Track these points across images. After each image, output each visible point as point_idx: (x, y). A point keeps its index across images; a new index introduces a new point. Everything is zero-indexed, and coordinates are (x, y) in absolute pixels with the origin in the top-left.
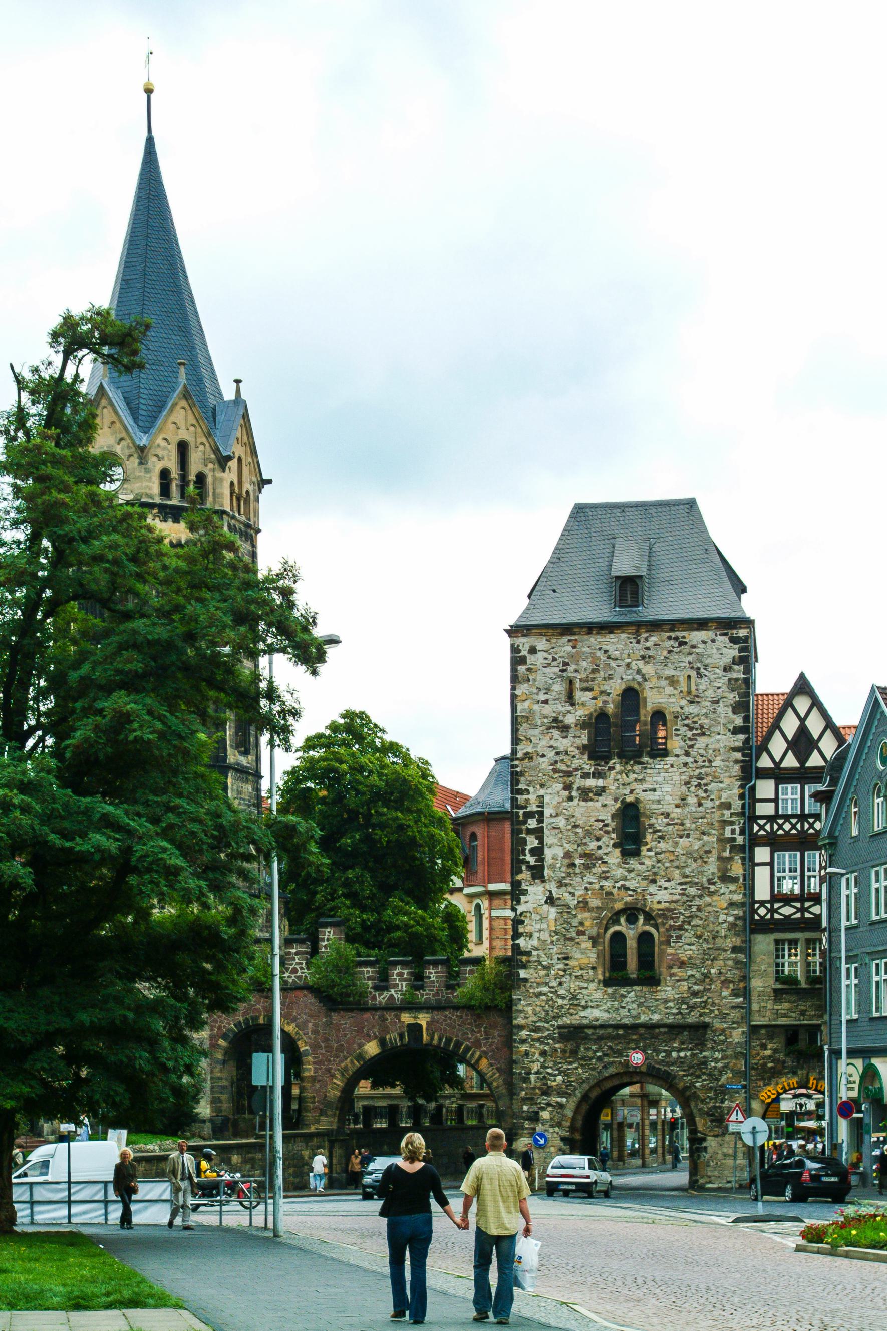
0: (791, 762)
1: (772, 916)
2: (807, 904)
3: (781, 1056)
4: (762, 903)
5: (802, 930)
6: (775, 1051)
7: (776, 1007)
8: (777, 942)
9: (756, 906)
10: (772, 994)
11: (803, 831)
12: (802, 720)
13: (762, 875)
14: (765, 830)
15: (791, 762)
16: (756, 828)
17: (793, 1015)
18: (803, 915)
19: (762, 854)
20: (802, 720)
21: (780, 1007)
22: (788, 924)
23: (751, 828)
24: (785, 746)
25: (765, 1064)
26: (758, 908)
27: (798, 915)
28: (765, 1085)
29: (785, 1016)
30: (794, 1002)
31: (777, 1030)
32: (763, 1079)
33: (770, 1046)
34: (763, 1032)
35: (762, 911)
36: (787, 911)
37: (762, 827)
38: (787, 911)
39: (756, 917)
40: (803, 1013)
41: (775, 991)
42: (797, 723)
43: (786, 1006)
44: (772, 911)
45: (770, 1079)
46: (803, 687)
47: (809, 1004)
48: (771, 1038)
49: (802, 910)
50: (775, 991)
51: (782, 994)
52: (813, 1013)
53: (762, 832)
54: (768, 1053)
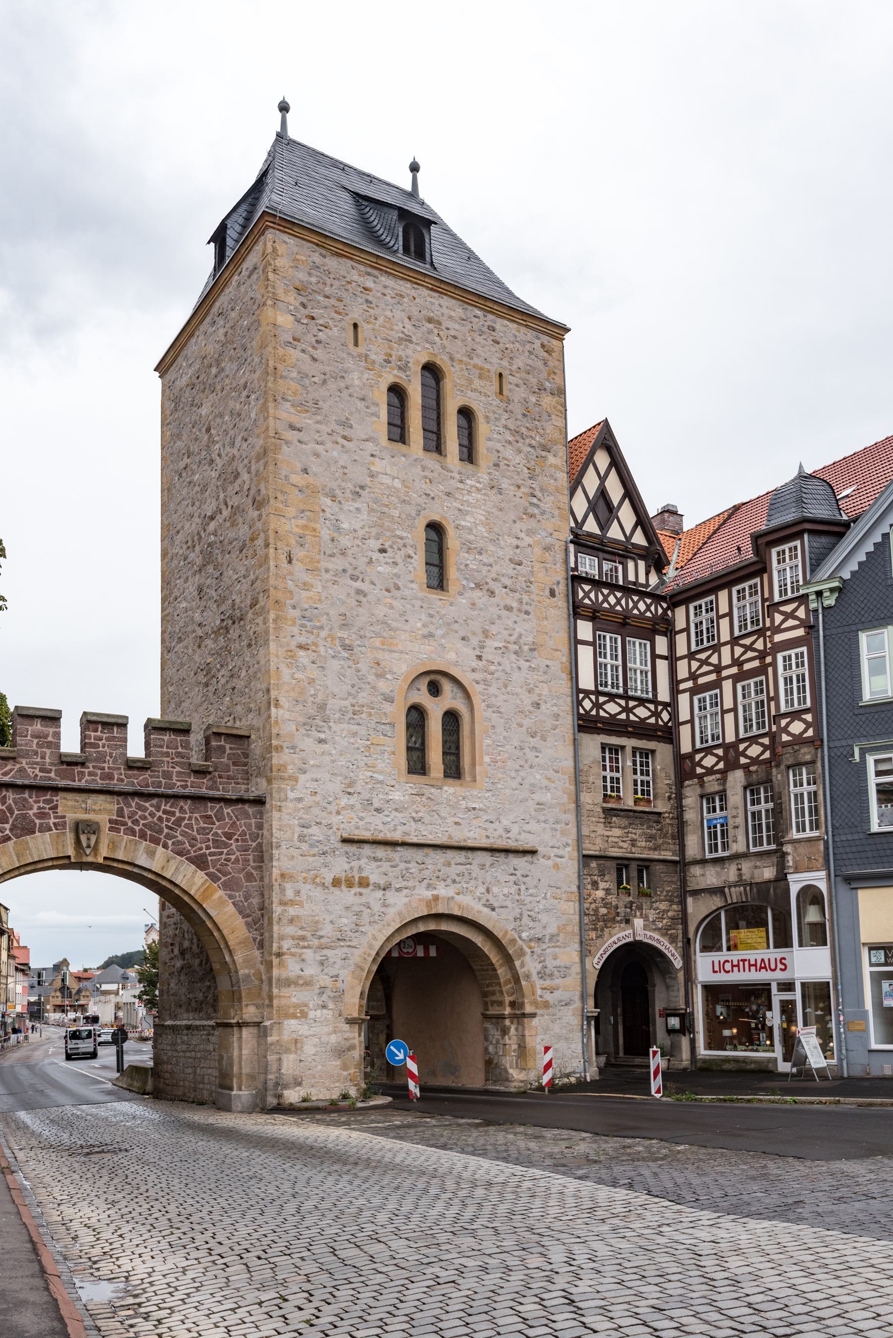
0: (591, 526)
1: (598, 712)
2: (632, 704)
3: (612, 899)
4: (587, 693)
5: (629, 735)
6: (607, 891)
7: (607, 833)
8: (604, 747)
9: (581, 696)
10: (602, 815)
11: (626, 610)
12: (603, 479)
13: (585, 654)
14: (590, 599)
15: (591, 526)
16: (581, 594)
17: (625, 845)
18: (628, 716)
19: (585, 630)
20: (603, 479)
21: (609, 833)
22: (612, 726)
23: (574, 593)
24: (586, 505)
25: (596, 910)
26: (583, 699)
27: (623, 716)
28: (597, 937)
29: (615, 845)
30: (624, 828)
31: (609, 864)
32: (595, 929)
33: (602, 885)
34: (594, 864)
35: (587, 704)
36: (612, 708)
37: (587, 595)
38: (612, 708)
39: (582, 711)
40: (633, 843)
41: (605, 810)
42: (597, 482)
43: (617, 832)
44: (597, 706)
45: (602, 930)
46: (604, 438)
47: (639, 832)
48: (602, 874)
49: (627, 710)
50: (605, 810)
51: (612, 816)
52: (643, 844)
53: (587, 601)
54: (600, 894)
